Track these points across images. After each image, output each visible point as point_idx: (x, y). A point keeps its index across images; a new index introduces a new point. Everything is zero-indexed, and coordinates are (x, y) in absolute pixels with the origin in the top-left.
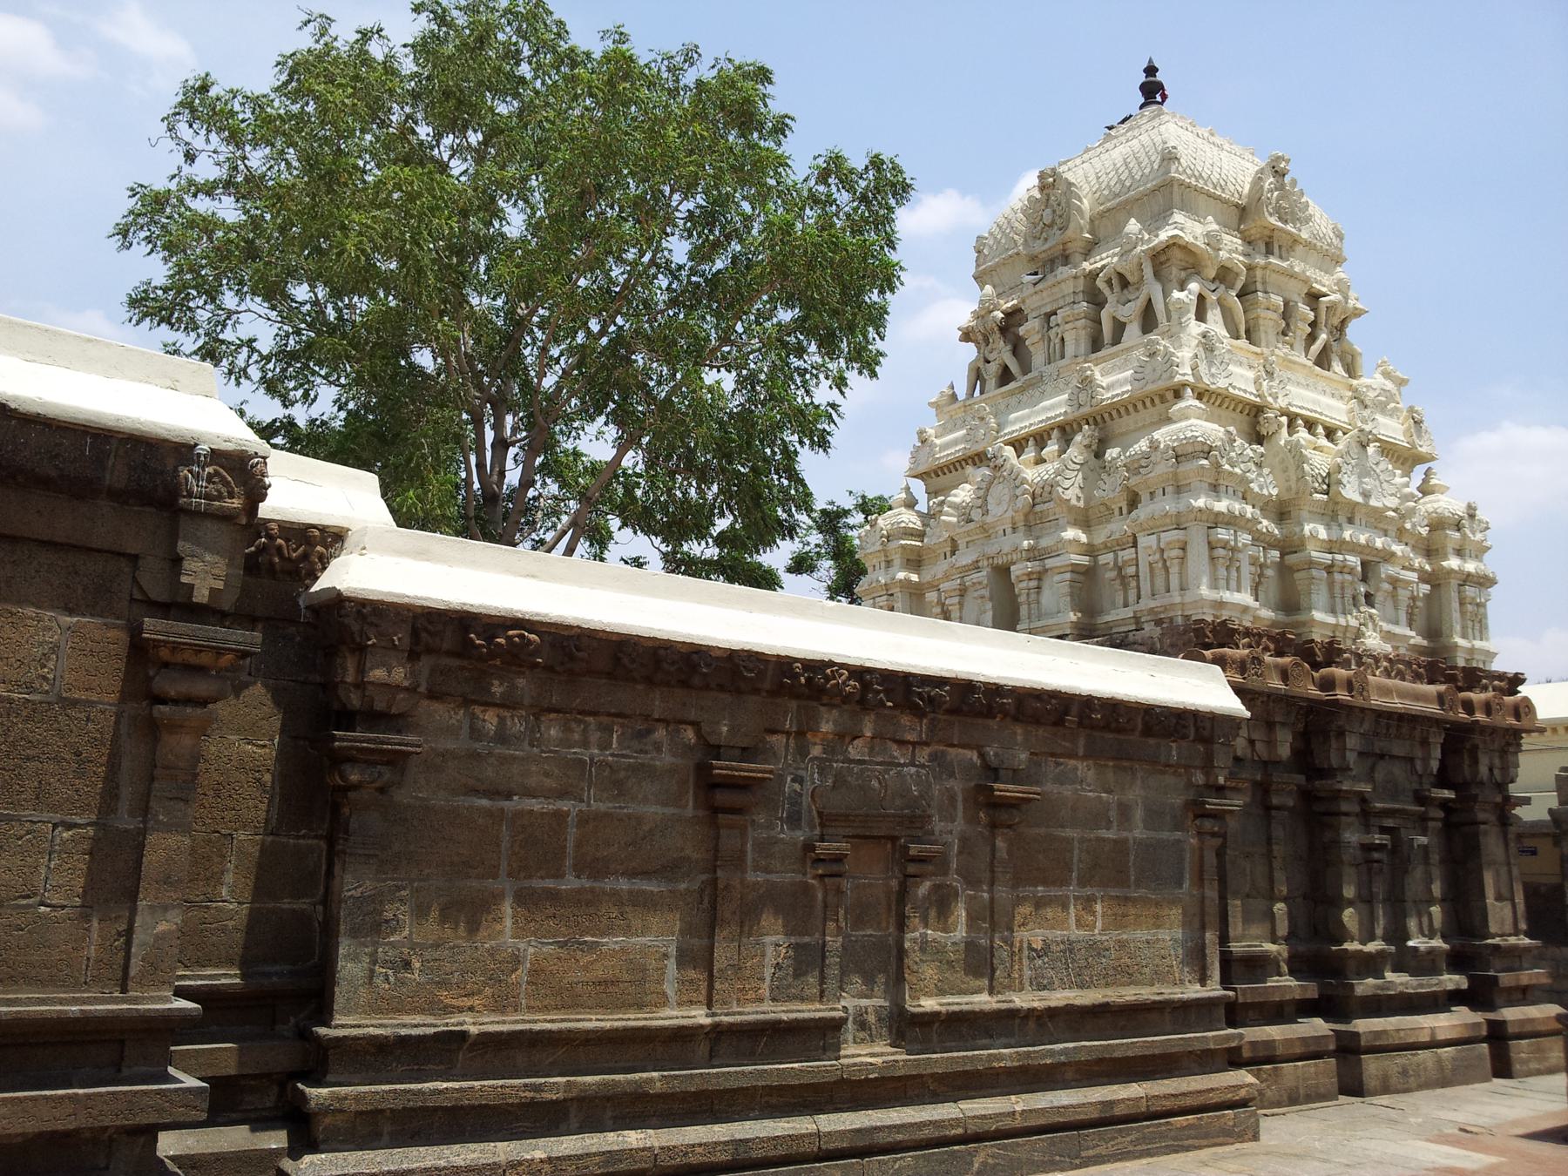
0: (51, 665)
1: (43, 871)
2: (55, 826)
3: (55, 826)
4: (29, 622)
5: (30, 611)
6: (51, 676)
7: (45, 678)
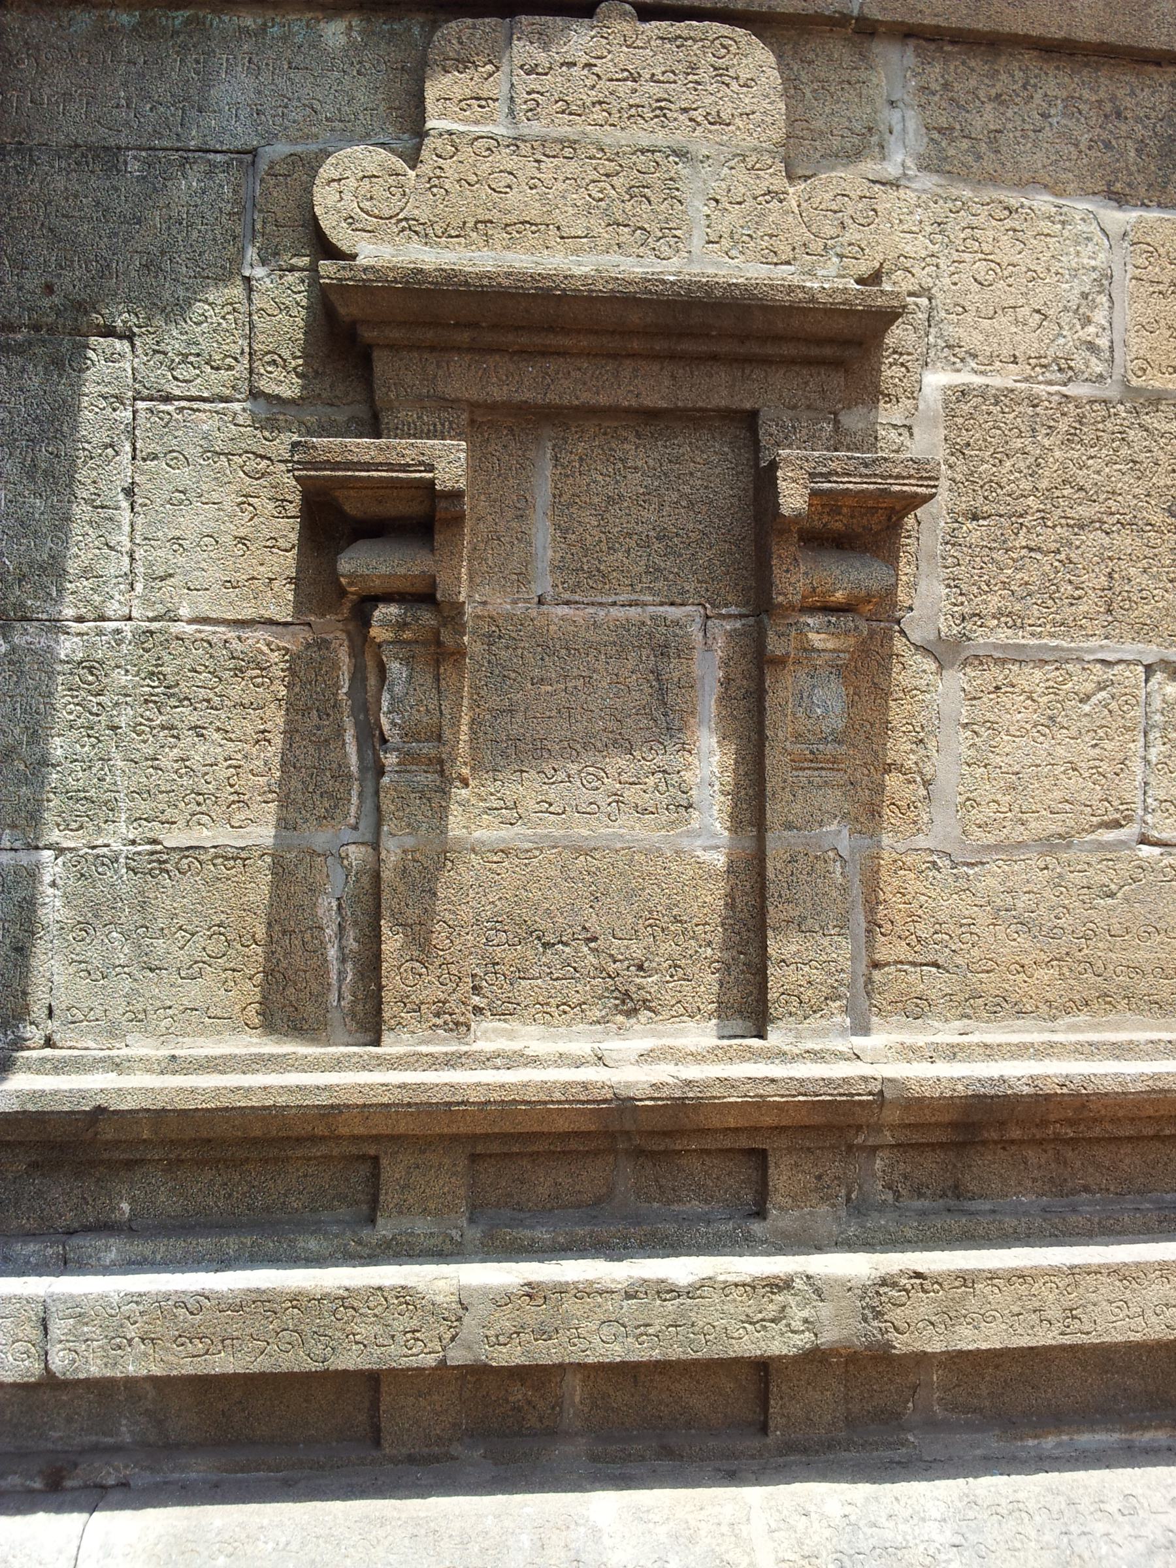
0: (1100, 317)
1: (1137, 766)
2: (1149, 669)
3: (1149, 669)
4: (1045, 226)
5: (1043, 202)
6: (1103, 342)
7: (1092, 347)
